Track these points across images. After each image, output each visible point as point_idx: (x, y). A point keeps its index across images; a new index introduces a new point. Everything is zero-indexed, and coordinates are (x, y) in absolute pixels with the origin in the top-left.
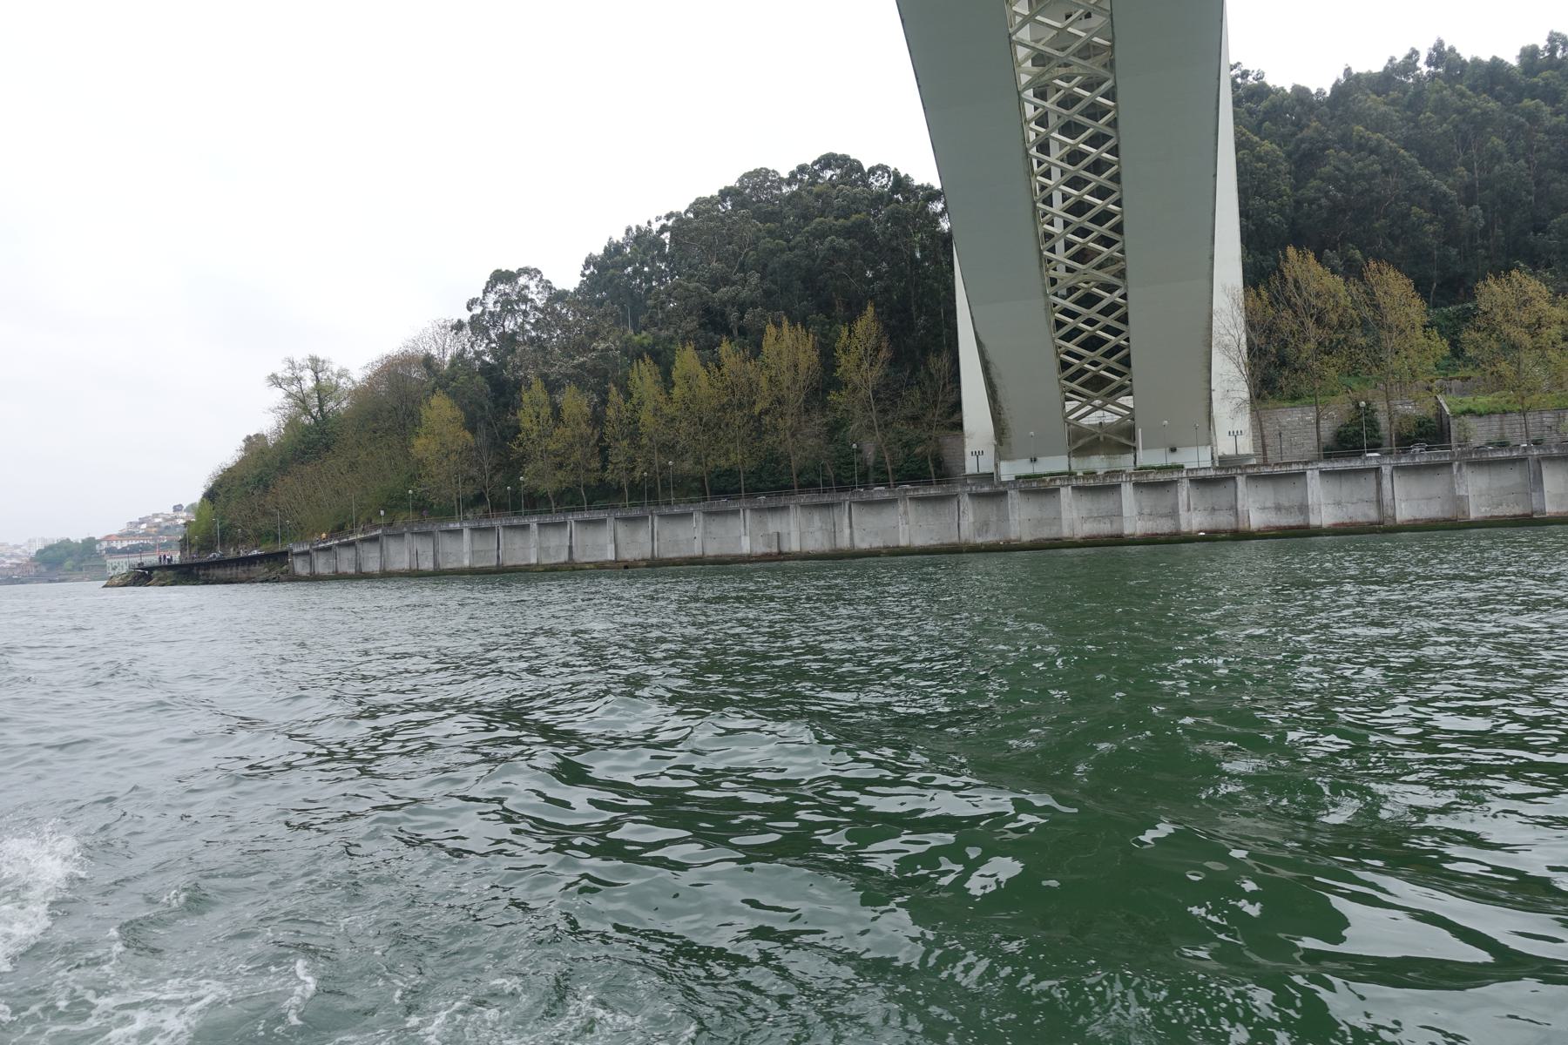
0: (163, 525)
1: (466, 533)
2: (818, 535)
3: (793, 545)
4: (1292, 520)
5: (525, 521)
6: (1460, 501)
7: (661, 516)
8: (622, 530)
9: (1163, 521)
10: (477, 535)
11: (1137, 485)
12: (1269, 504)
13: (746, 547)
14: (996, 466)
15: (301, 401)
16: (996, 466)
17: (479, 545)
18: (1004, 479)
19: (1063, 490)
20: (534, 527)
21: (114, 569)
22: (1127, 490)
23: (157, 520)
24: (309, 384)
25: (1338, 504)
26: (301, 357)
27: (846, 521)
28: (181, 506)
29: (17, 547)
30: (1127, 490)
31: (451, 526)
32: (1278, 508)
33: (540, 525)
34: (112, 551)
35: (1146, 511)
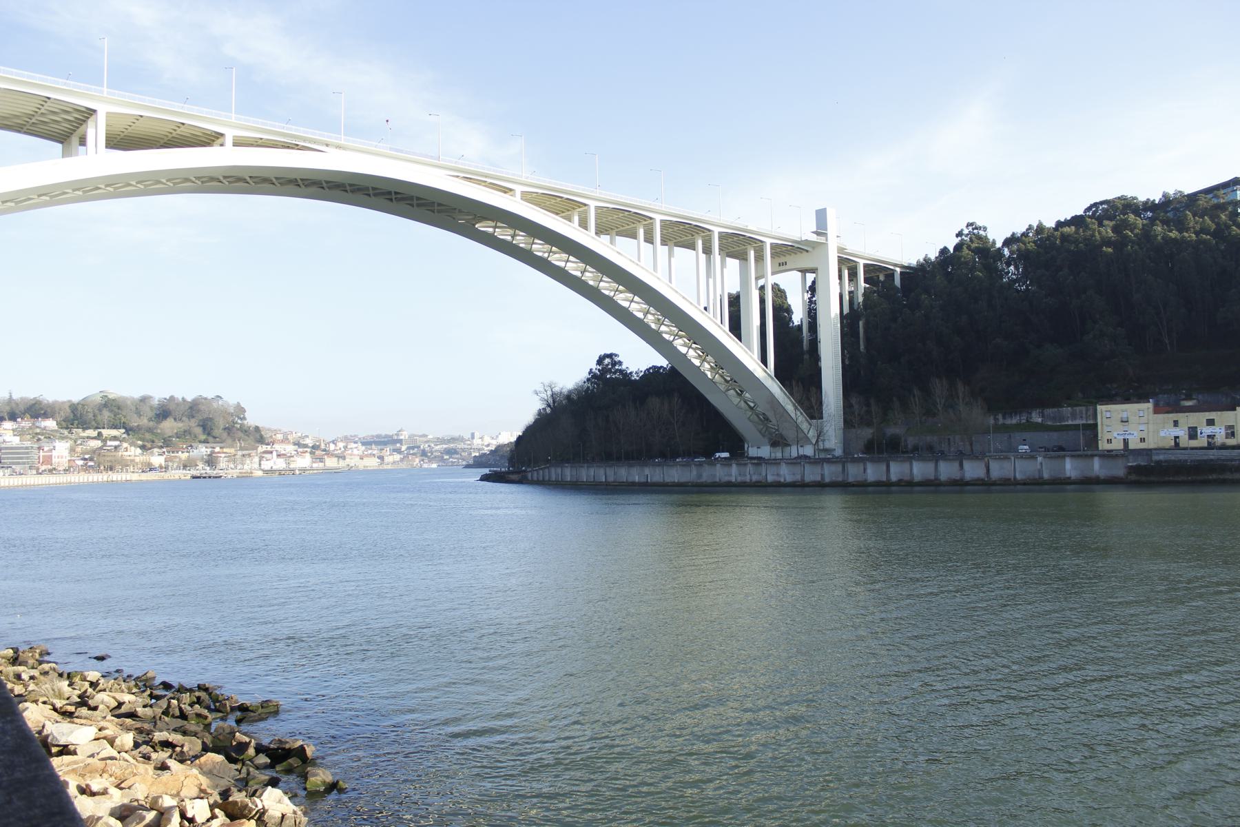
8: (608, 469)
25: (794, 474)
26: (547, 383)
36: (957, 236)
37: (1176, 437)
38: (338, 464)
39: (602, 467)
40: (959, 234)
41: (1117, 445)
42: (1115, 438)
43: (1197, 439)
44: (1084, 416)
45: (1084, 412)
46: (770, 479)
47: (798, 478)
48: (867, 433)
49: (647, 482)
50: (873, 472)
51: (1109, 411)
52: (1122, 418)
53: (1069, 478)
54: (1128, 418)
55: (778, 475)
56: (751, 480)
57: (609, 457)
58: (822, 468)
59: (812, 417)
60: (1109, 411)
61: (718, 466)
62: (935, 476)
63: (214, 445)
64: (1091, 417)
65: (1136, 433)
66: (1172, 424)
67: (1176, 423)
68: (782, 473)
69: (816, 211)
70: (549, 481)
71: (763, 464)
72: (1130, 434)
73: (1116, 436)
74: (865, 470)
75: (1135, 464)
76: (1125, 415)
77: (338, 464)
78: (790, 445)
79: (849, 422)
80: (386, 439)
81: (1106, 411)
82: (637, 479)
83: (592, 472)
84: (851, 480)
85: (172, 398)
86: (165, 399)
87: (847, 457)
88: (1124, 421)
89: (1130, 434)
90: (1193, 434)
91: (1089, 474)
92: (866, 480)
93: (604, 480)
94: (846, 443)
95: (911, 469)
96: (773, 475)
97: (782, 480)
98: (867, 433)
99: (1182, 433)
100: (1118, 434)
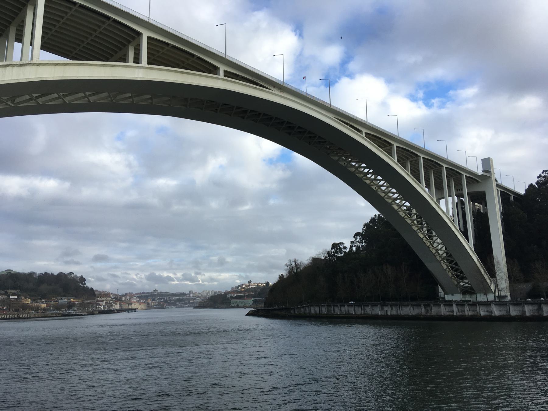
0: (247, 288)
1: (326, 306)
2: (394, 311)
6: (524, 312)
8: (356, 308)
11: (457, 305)
14: (444, 296)
15: (292, 269)
16: (444, 296)
18: (446, 299)
19: (441, 305)
21: (233, 303)
22: (454, 306)
23: (244, 286)
24: (294, 264)
25: (500, 311)
26: (292, 259)
27: (399, 309)
28: (251, 281)
29: (199, 293)
30: (454, 306)
34: (232, 298)
36: (538, 177)
38: (128, 307)
40: (540, 176)
46: (482, 314)
47: (504, 313)
48: (526, 287)
49: (387, 314)
50: (529, 310)
55: (491, 312)
56: (468, 314)
57: (361, 301)
59: (492, 278)
63: (69, 298)
69: (482, 159)
77: (128, 307)
78: (476, 294)
79: (512, 279)
80: (147, 295)
82: (380, 313)
83: (343, 309)
85: (46, 273)
86: (42, 274)
87: (515, 302)
93: (354, 314)
94: (512, 292)
96: (484, 311)
98: (526, 287)
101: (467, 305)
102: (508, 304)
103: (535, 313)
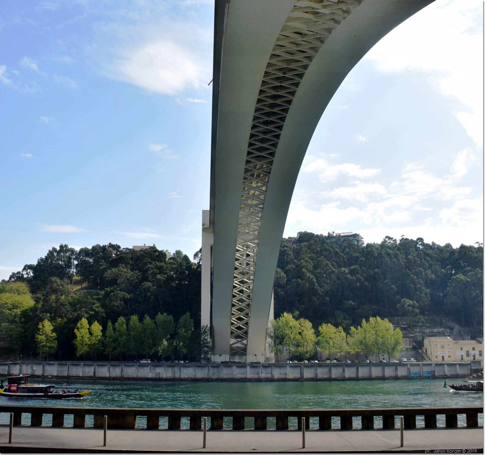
3: (164, 376)
4: (283, 376)
5: (81, 363)
6: (316, 374)
7: (125, 365)
8: (111, 369)
9: (256, 375)
10: (59, 366)
11: (251, 366)
12: (279, 373)
13: (150, 375)
17: (59, 369)
19: (234, 367)
20: (82, 365)
31: (51, 362)
32: (280, 374)
33: (84, 365)
35: (252, 373)
37: (462, 356)
39: (106, 365)
41: (440, 359)
42: (439, 355)
43: (469, 356)
44: (405, 344)
45: (405, 342)
51: (436, 342)
52: (441, 346)
53: (447, 375)
54: (444, 345)
55: (286, 374)
58: (316, 370)
60: (436, 342)
61: (234, 367)
62: (383, 374)
64: (408, 344)
65: (447, 353)
66: (460, 349)
67: (462, 348)
68: (287, 372)
70: (43, 375)
71: (273, 366)
72: (445, 353)
73: (439, 354)
74: (344, 371)
75: (474, 368)
76: (442, 344)
81: (435, 342)
84: (333, 376)
88: (443, 347)
89: (445, 353)
90: (468, 355)
91: (454, 373)
92: (345, 377)
95: (370, 371)
97: (288, 377)
99: (464, 353)
100: (440, 354)
101: (261, 367)
102: (302, 367)
103: (324, 375)
